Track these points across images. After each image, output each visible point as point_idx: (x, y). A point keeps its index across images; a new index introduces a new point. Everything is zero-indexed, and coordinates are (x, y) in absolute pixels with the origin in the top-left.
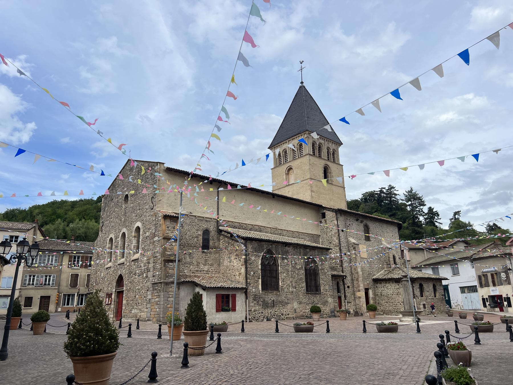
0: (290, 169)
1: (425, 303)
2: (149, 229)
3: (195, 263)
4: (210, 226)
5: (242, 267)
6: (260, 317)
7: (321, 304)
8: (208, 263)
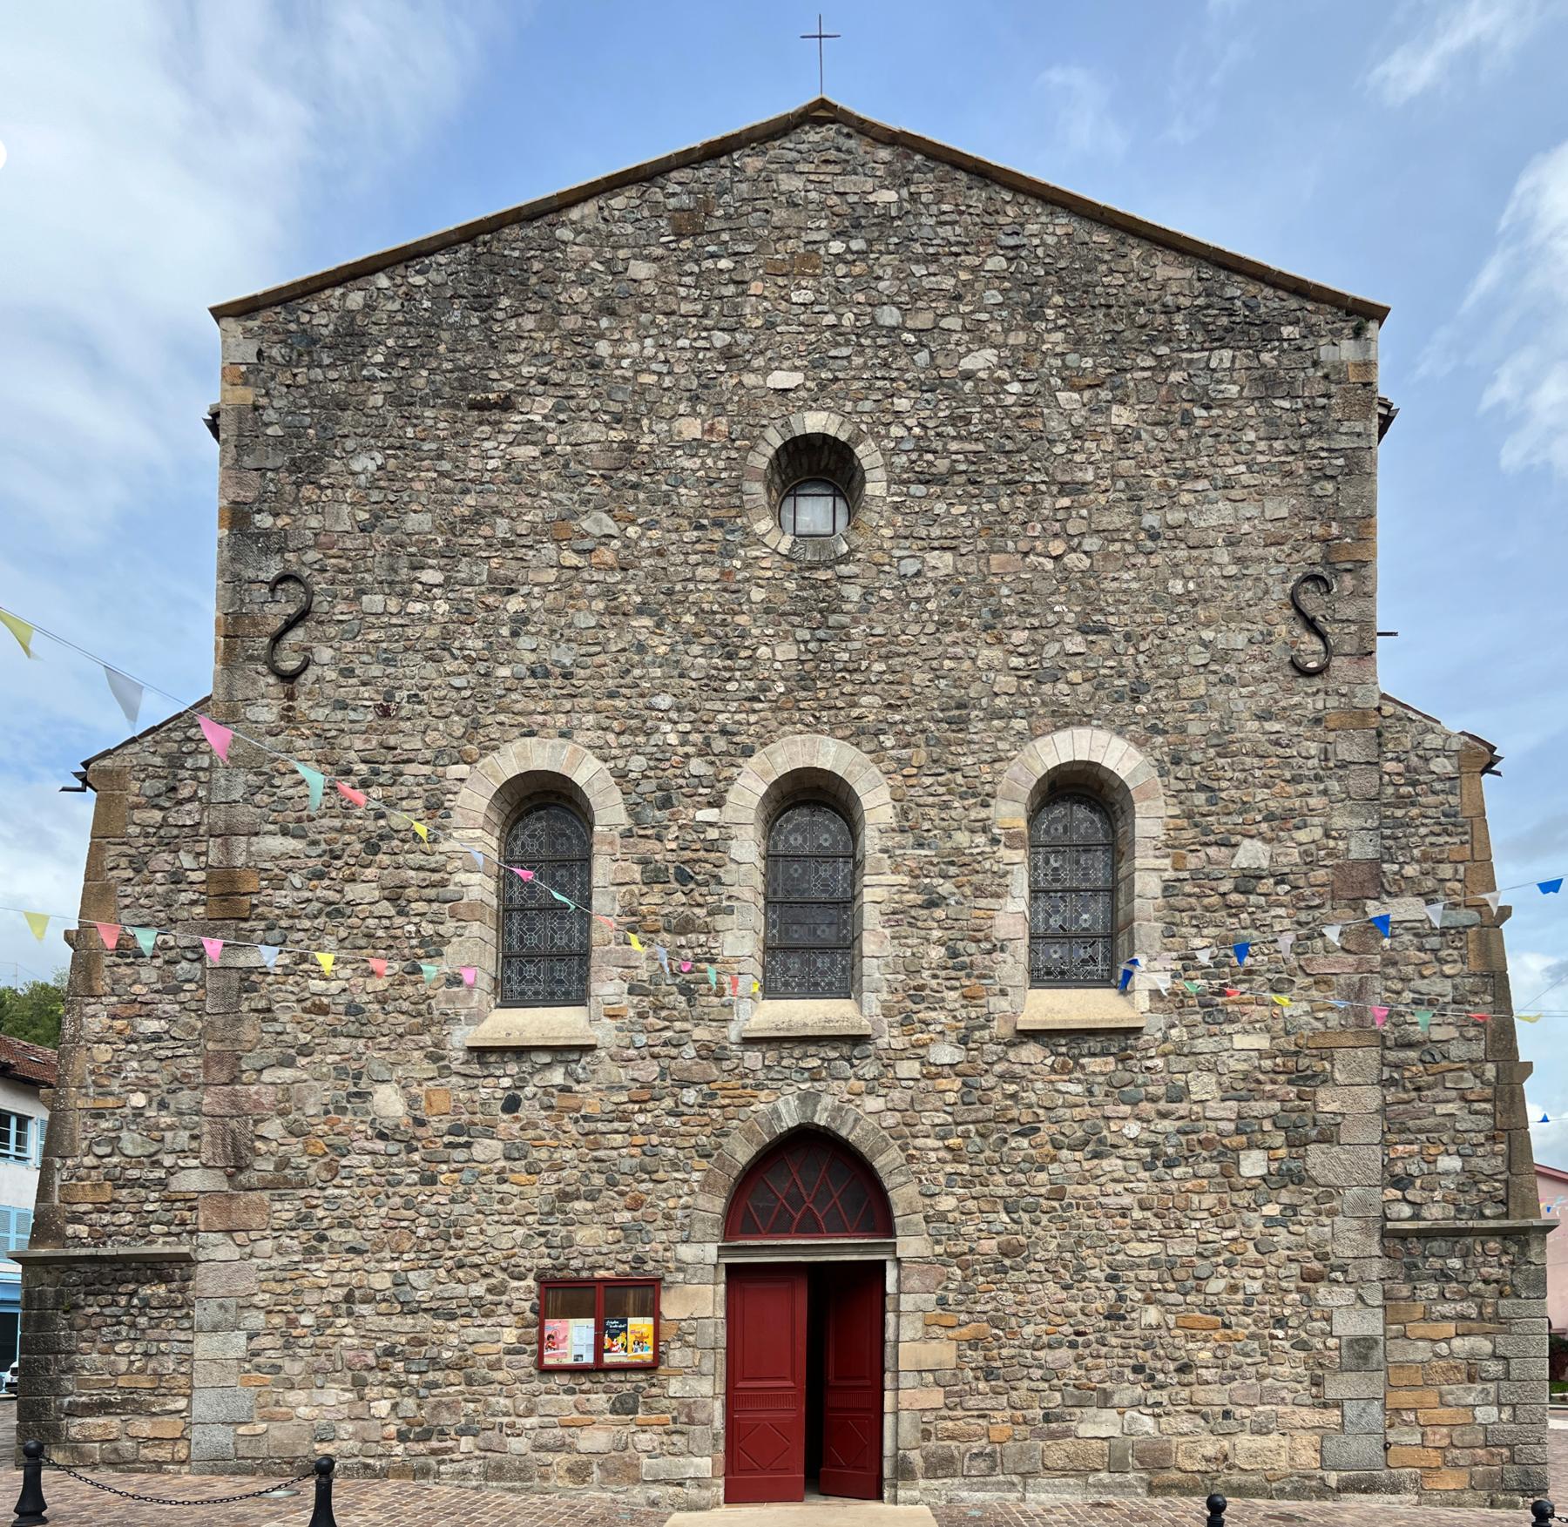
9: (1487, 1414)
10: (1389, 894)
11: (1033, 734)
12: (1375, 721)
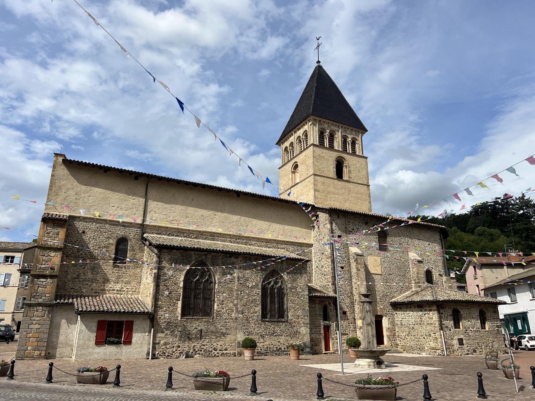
0: (296, 167)
1: (462, 336)
3: (100, 280)
4: (130, 233)
6: (174, 352)
7: (287, 336)
8: (123, 281)
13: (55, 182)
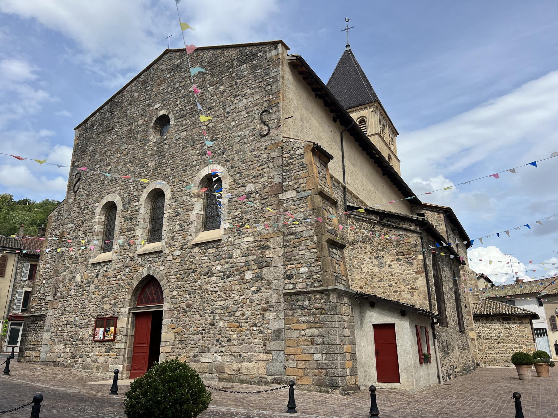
2: (260, 176)
5: (419, 276)
9: (318, 357)
10: (285, 191)
11: (200, 169)
12: (280, 145)
13: (285, 91)
